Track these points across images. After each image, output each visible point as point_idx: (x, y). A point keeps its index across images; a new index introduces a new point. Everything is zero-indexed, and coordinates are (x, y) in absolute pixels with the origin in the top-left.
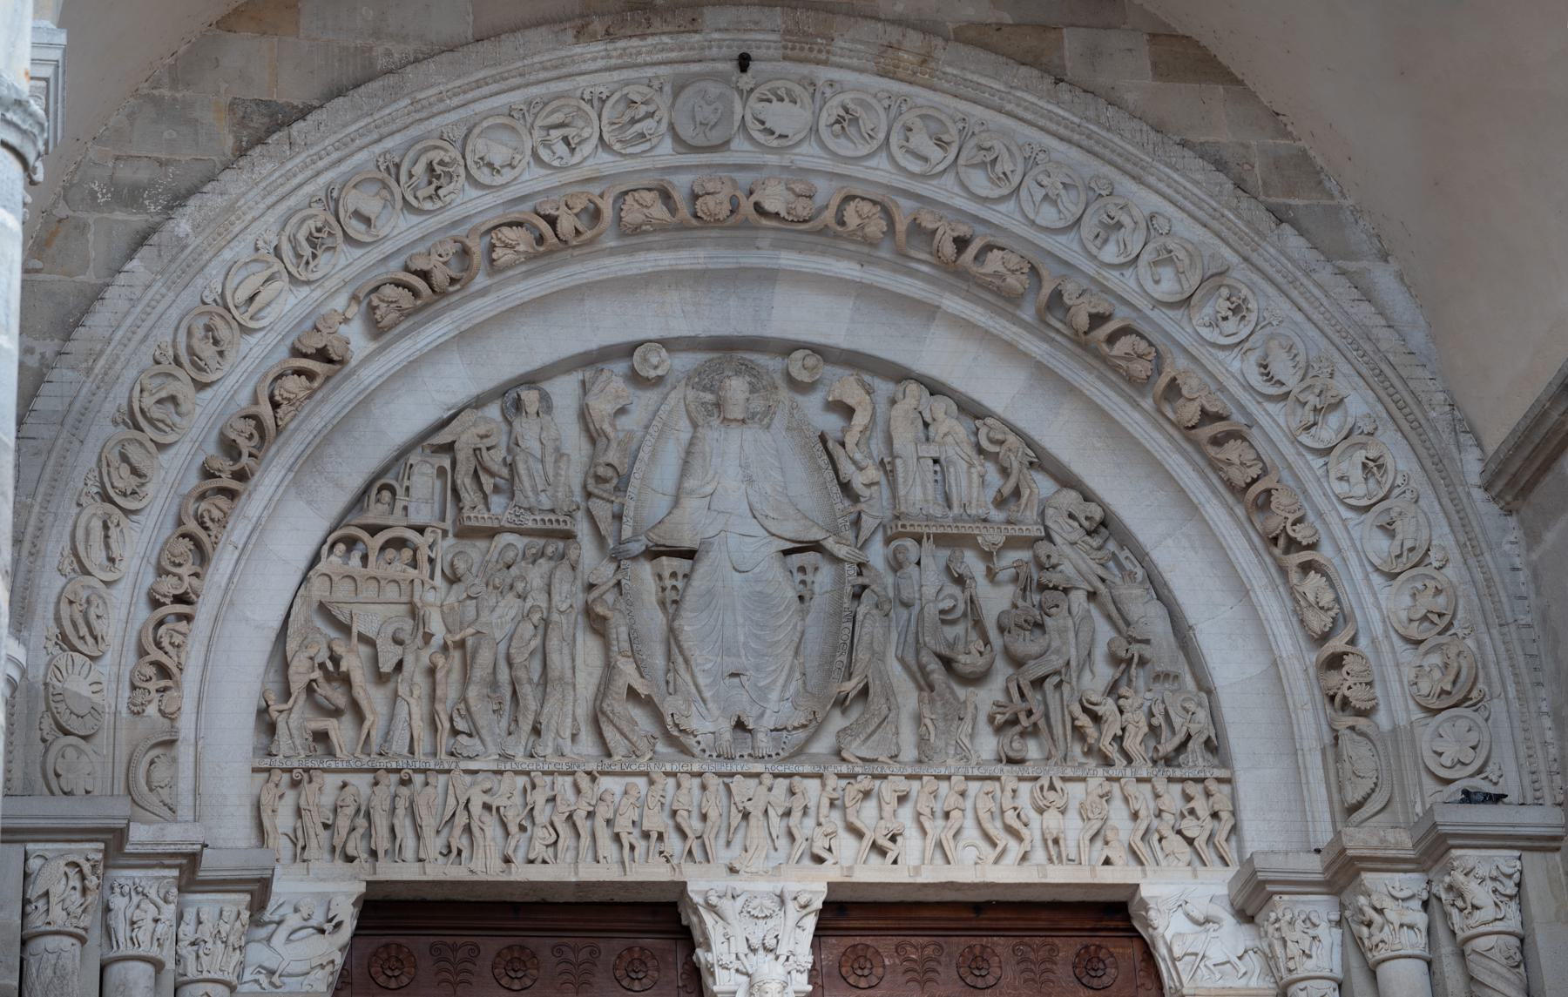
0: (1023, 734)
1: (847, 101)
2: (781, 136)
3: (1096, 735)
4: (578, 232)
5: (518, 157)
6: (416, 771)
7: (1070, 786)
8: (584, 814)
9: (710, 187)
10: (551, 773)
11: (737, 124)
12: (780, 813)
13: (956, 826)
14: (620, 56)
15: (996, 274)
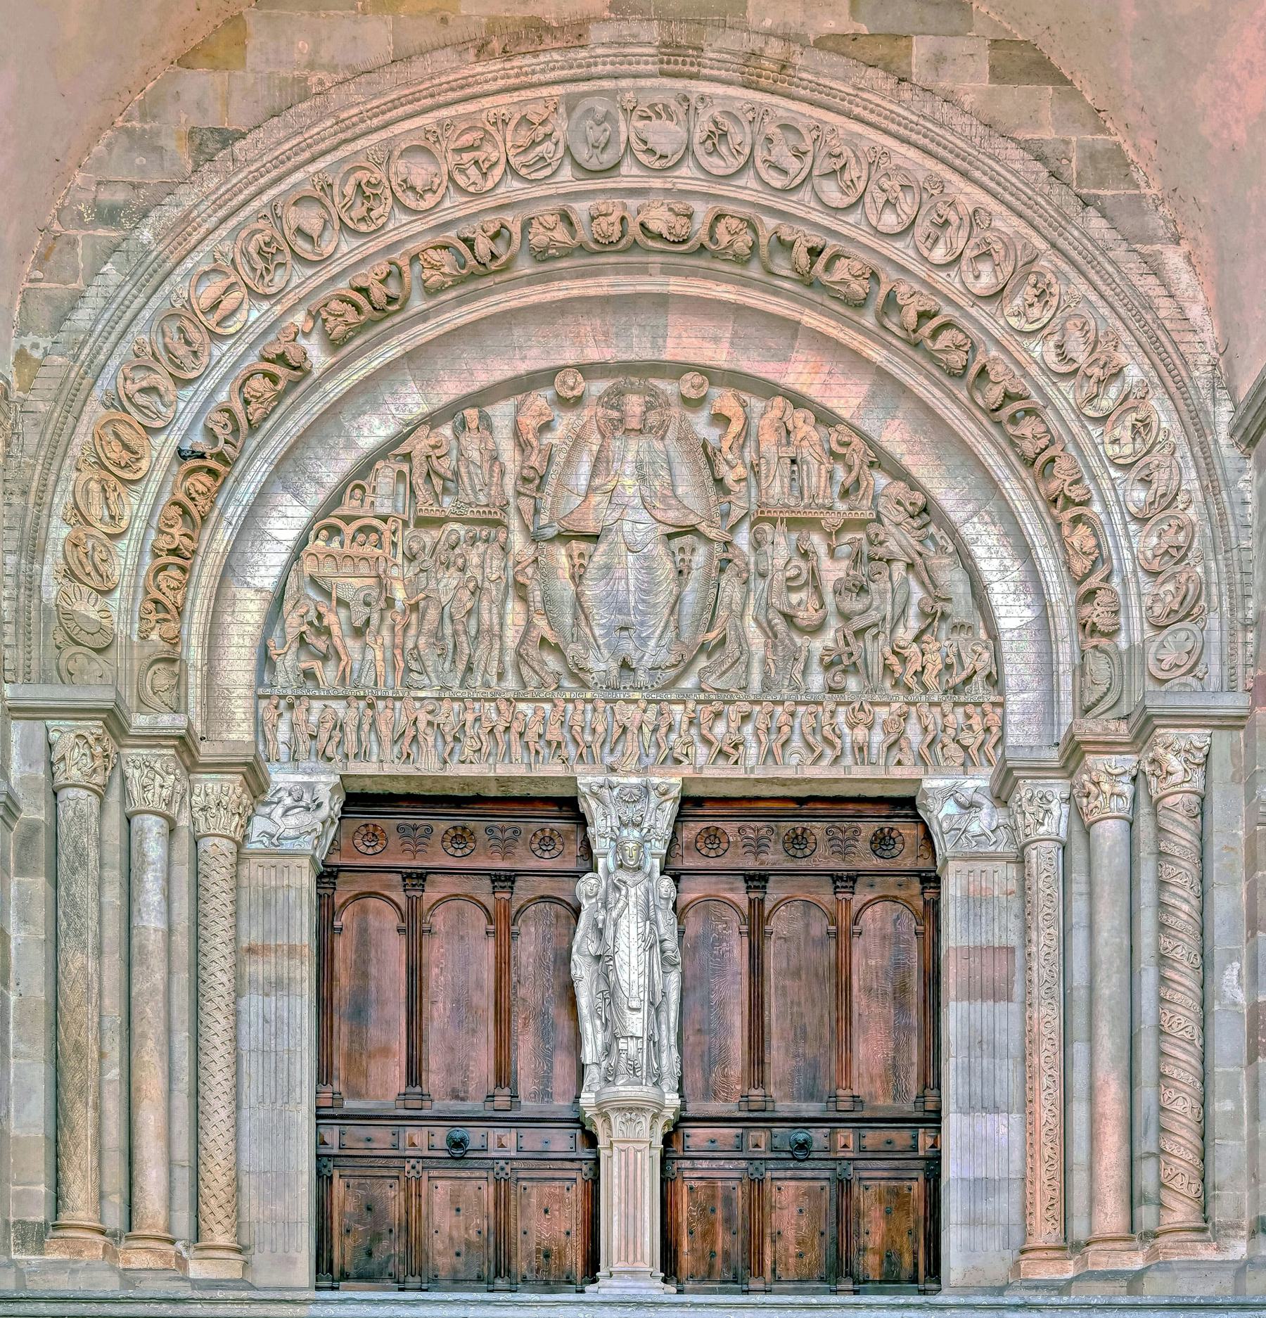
0: (844, 672)
1: (716, 114)
2: (661, 157)
3: (900, 671)
4: (494, 257)
5: (437, 181)
6: (378, 698)
7: (877, 709)
8: (502, 729)
9: (603, 209)
10: (478, 700)
11: (623, 146)
12: (651, 728)
13: (785, 738)
14: (517, 76)
15: (843, 282)
